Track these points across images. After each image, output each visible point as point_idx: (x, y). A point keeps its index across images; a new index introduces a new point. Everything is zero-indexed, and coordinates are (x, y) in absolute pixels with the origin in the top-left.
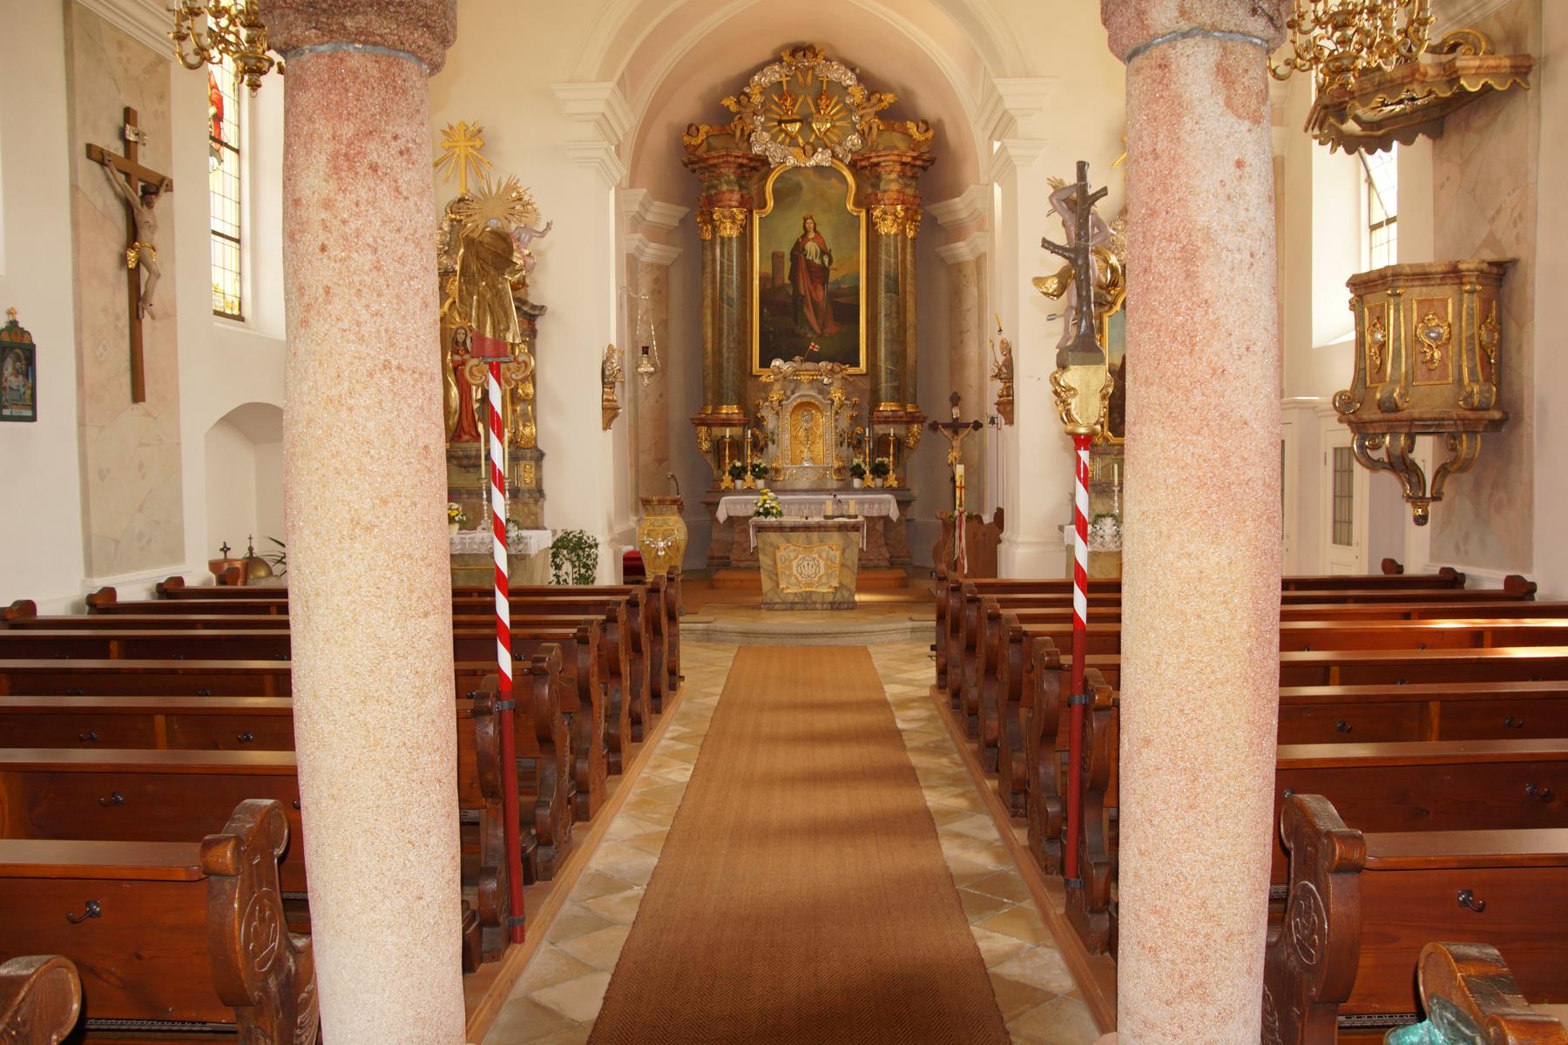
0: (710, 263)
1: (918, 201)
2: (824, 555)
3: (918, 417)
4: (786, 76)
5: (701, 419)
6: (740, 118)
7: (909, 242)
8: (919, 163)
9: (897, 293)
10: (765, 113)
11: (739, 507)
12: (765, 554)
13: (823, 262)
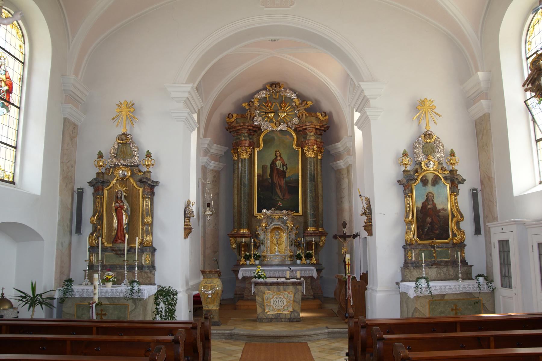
0: (237, 169)
1: (322, 144)
2: (286, 296)
3: (324, 233)
4: (268, 95)
5: (232, 234)
6: (250, 111)
7: (319, 161)
8: (322, 128)
9: (314, 182)
10: (259, 109)
11: (247, 272)
13: (283, 169)
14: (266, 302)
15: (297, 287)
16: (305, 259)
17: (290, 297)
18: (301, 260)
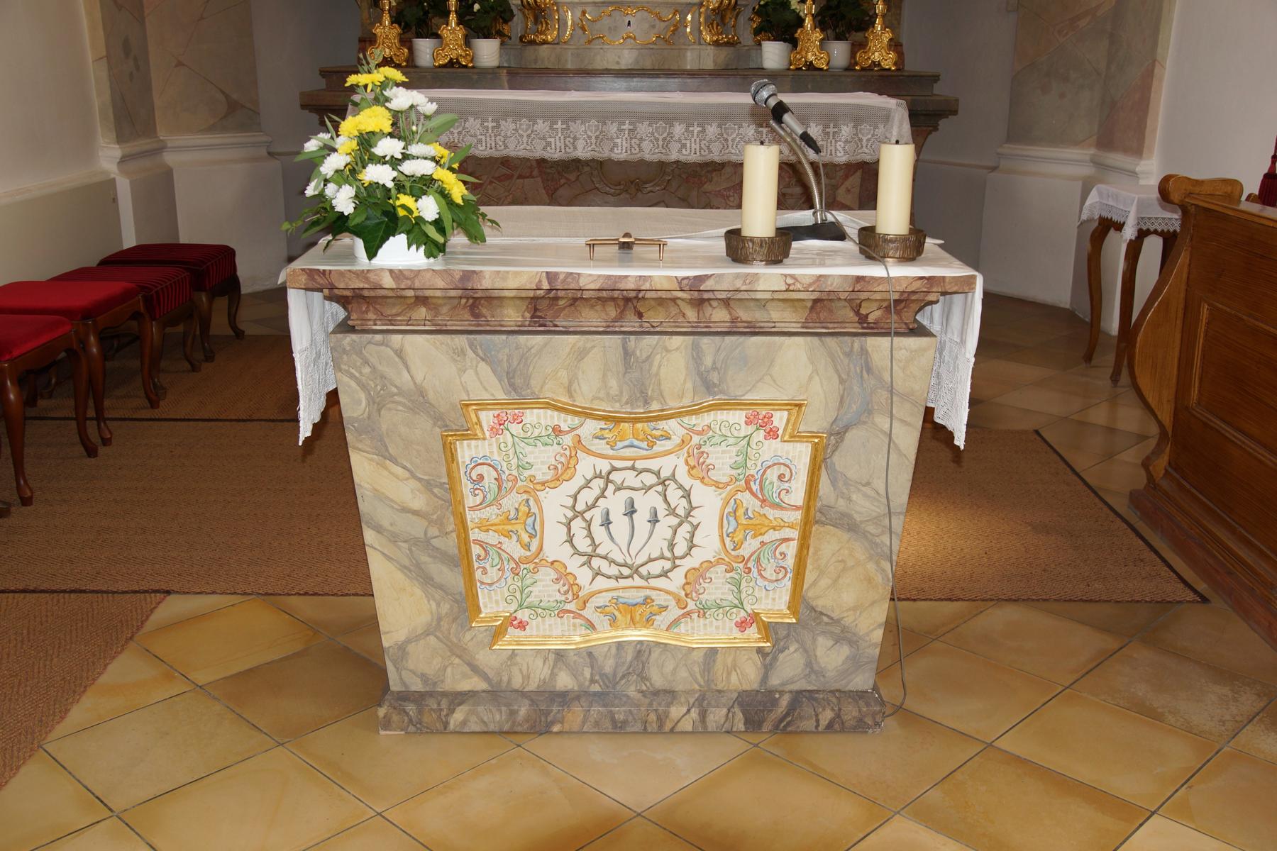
2: (722, 460)
12: (384, 454)
14: (485, 526)
15: (864, 351)
16: (818, 35)
17: (772, 475)
18: (793, 42)
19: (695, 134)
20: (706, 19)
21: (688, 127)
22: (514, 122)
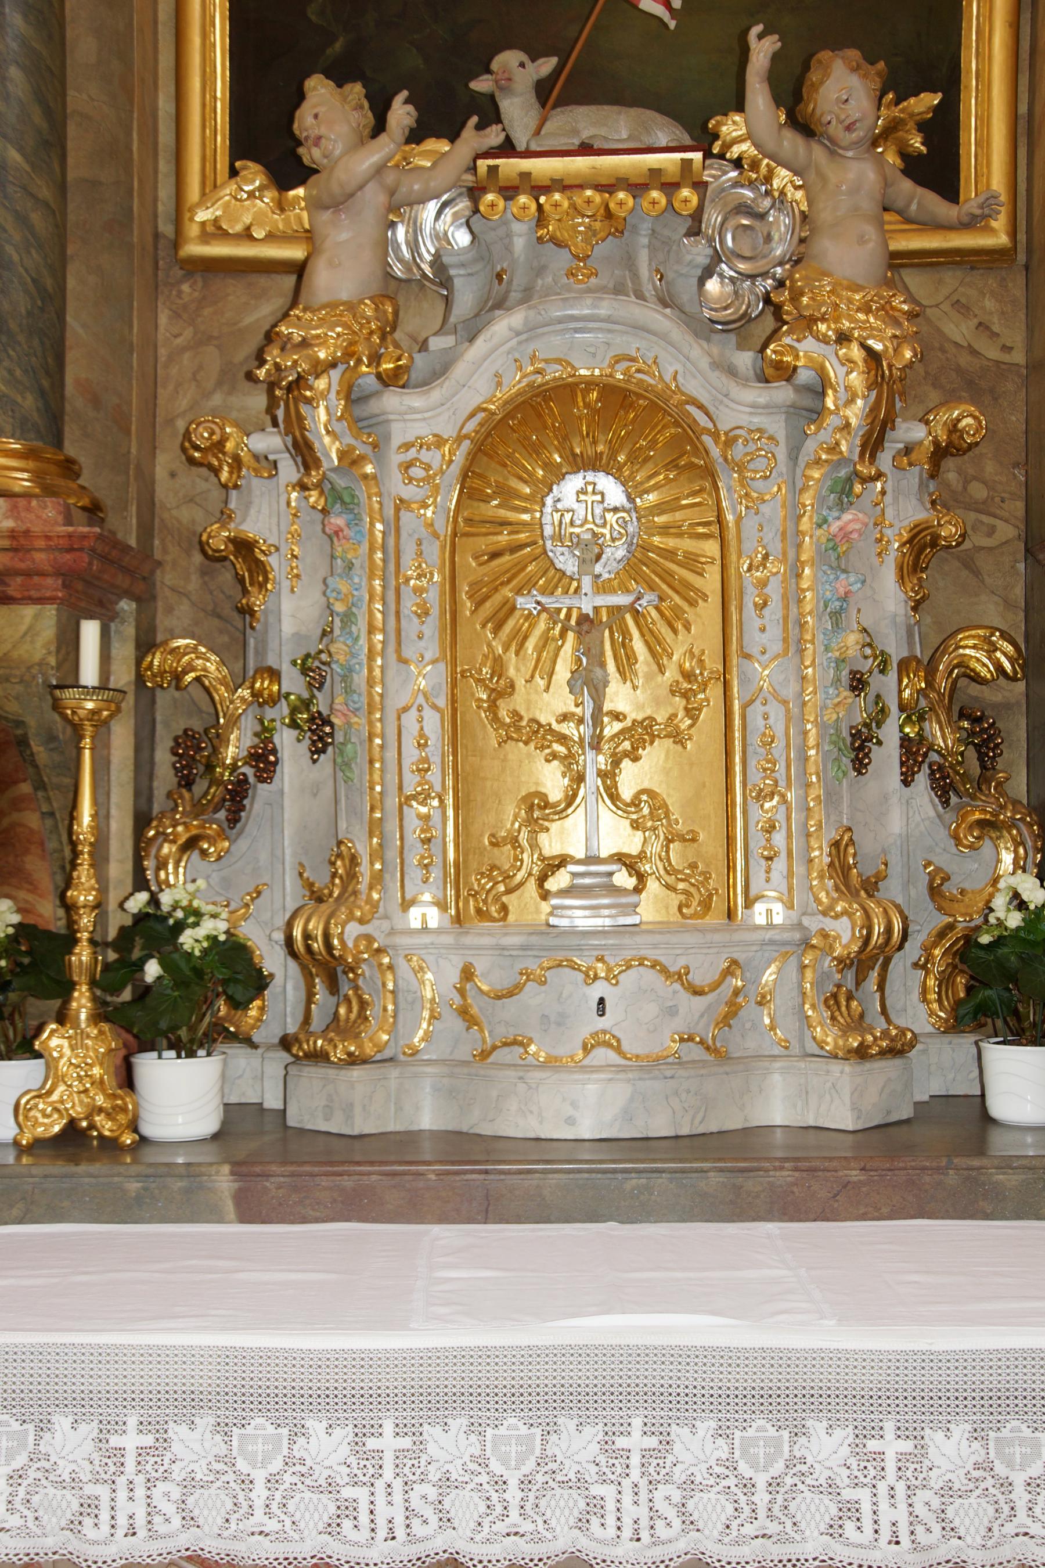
19: (891, 1466)
20: (817, 984)
21: (861, 1436)
22: (223, 1429)
